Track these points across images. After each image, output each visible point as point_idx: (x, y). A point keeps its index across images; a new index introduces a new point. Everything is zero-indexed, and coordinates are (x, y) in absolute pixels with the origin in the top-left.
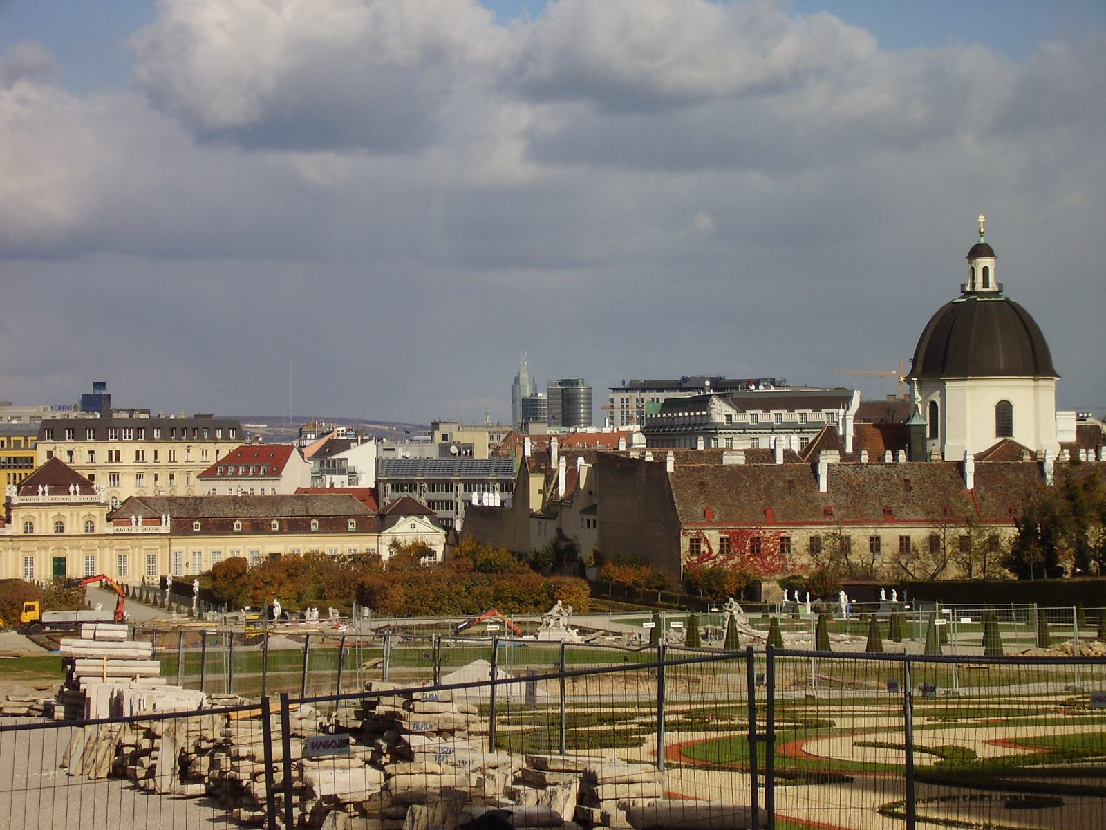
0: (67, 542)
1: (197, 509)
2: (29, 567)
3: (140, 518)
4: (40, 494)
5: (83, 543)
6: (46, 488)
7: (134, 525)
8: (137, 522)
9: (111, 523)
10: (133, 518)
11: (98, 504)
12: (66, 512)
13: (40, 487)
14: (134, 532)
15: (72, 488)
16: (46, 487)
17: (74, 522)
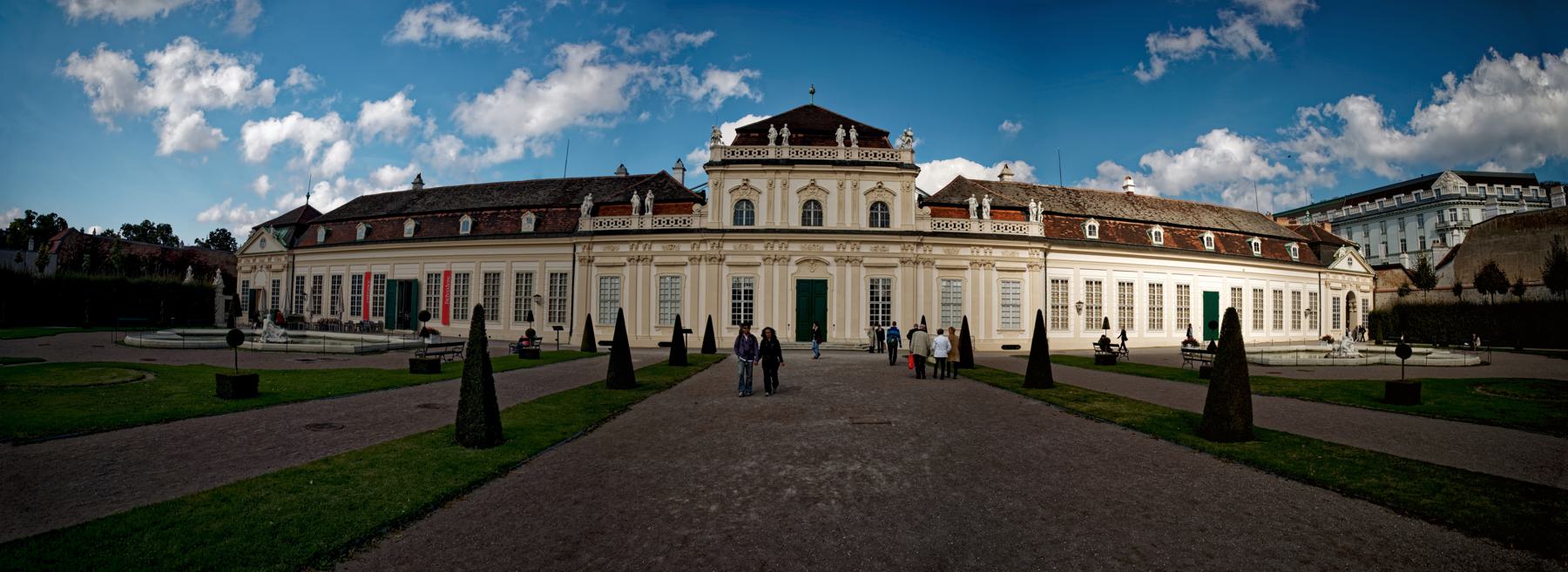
0: (831, 248)
1: (1078, 205)
2: (743, 301)
3: (986, 202)
4: (772, 144)
5: (866, 249)
6: (785, 132)
7: (974, 217)
8: (980, 208)
9: (927, 209)
10: (973, 202)
11: (900, 165)
12: (829, 182)
13: (772, 129)
14: (975, 228)
15: (840, 132)
16: (785, 129)
17: (846, 201)
